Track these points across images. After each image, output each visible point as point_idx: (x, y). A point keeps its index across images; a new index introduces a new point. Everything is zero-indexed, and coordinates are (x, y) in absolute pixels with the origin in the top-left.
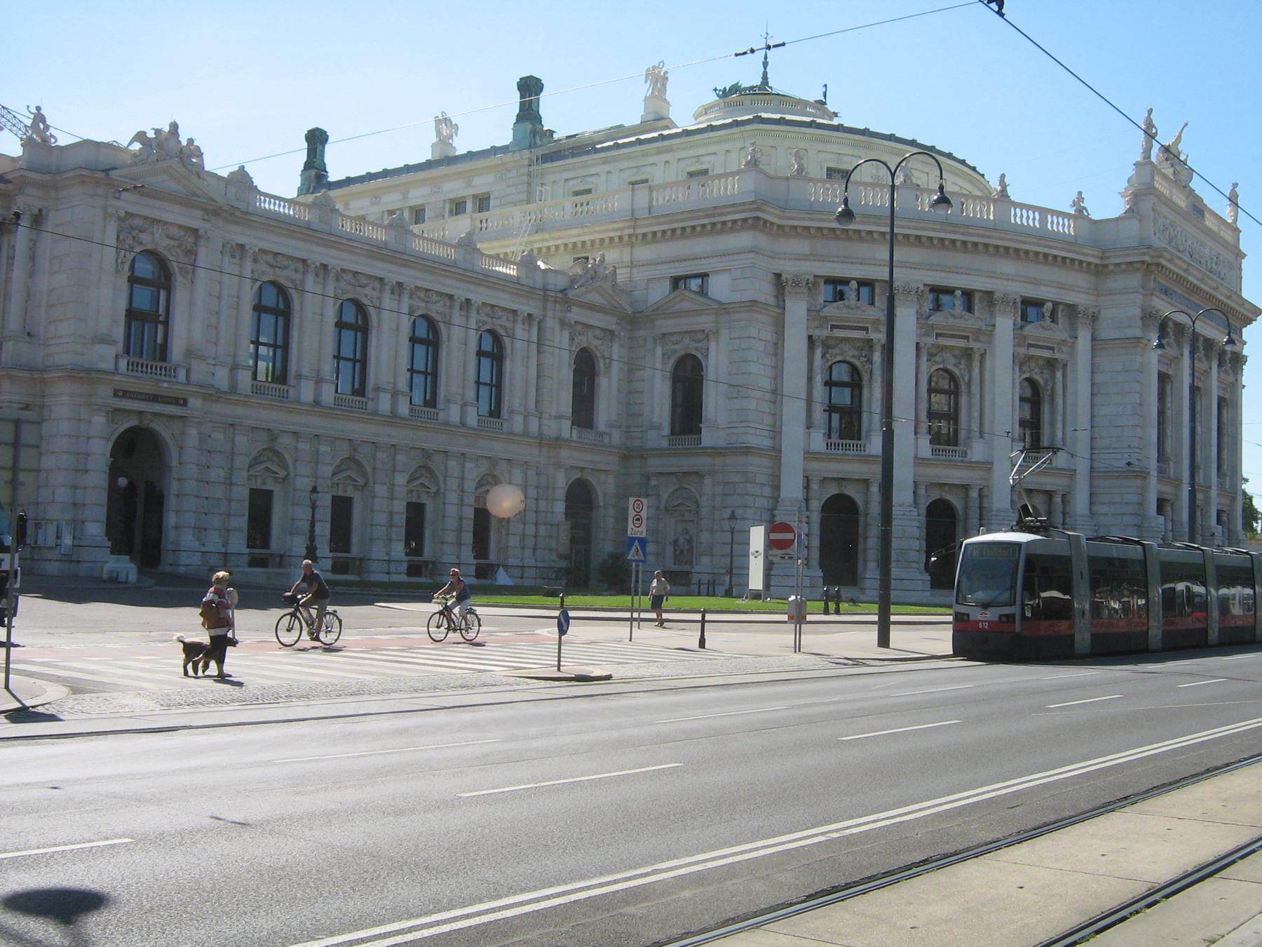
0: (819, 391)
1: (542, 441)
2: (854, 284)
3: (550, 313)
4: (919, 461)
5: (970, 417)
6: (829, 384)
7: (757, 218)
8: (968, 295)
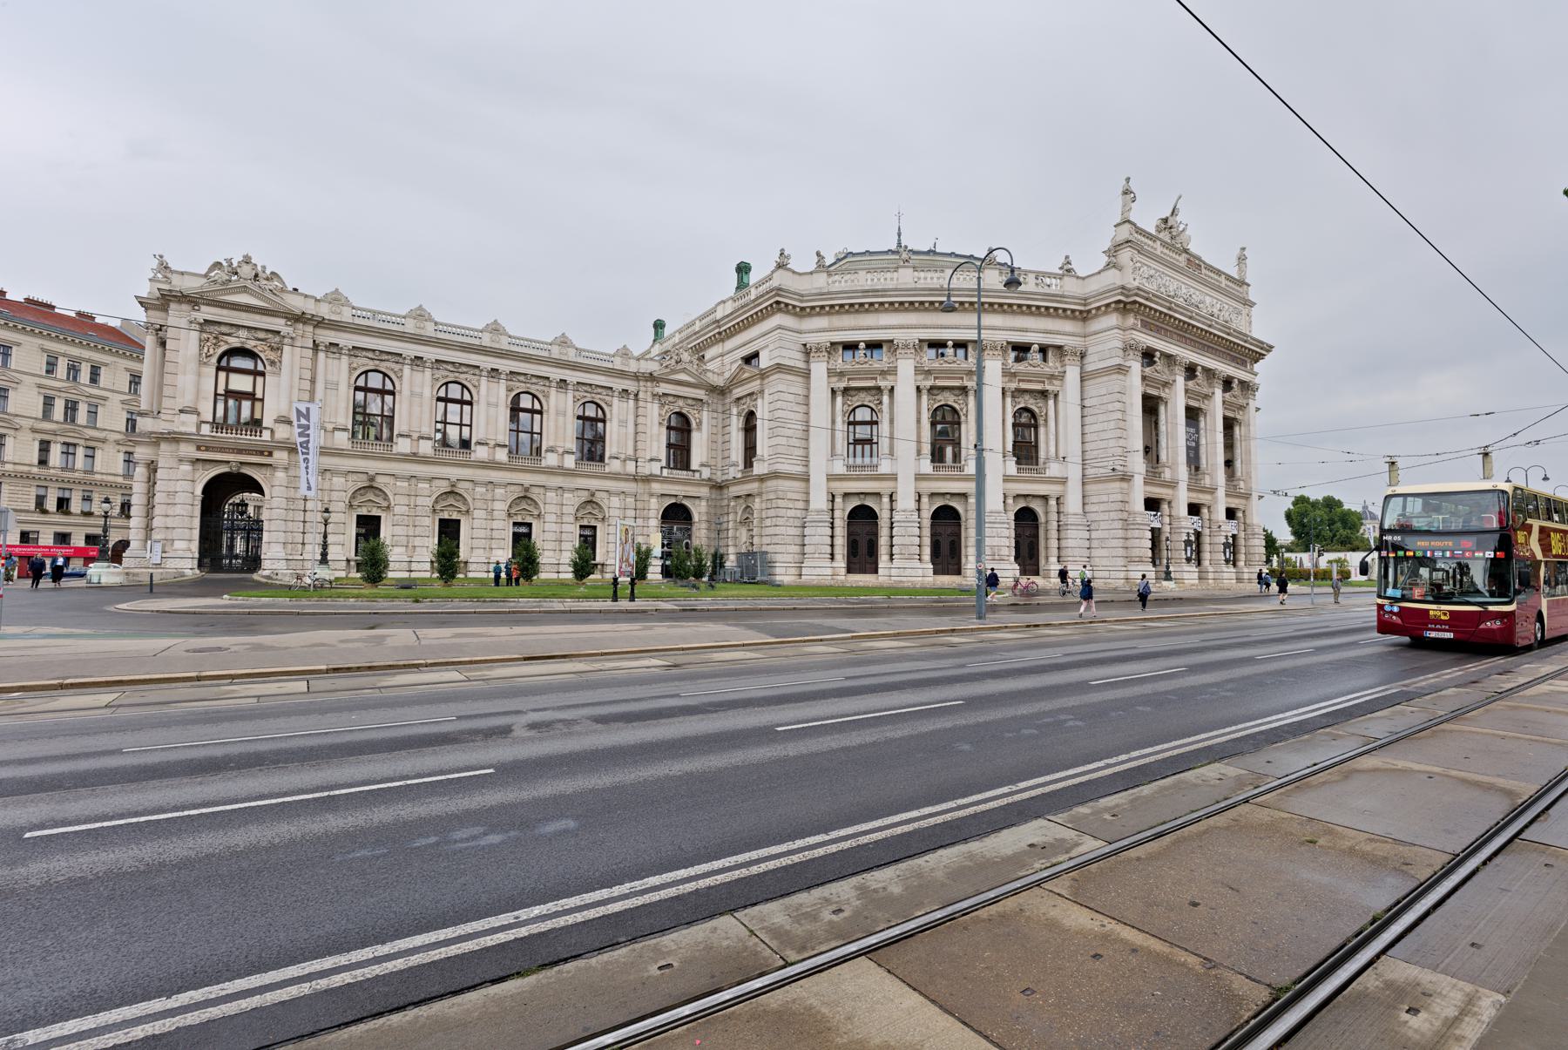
1: (635, 478)
4: (919, 477)
7: (778, 303)
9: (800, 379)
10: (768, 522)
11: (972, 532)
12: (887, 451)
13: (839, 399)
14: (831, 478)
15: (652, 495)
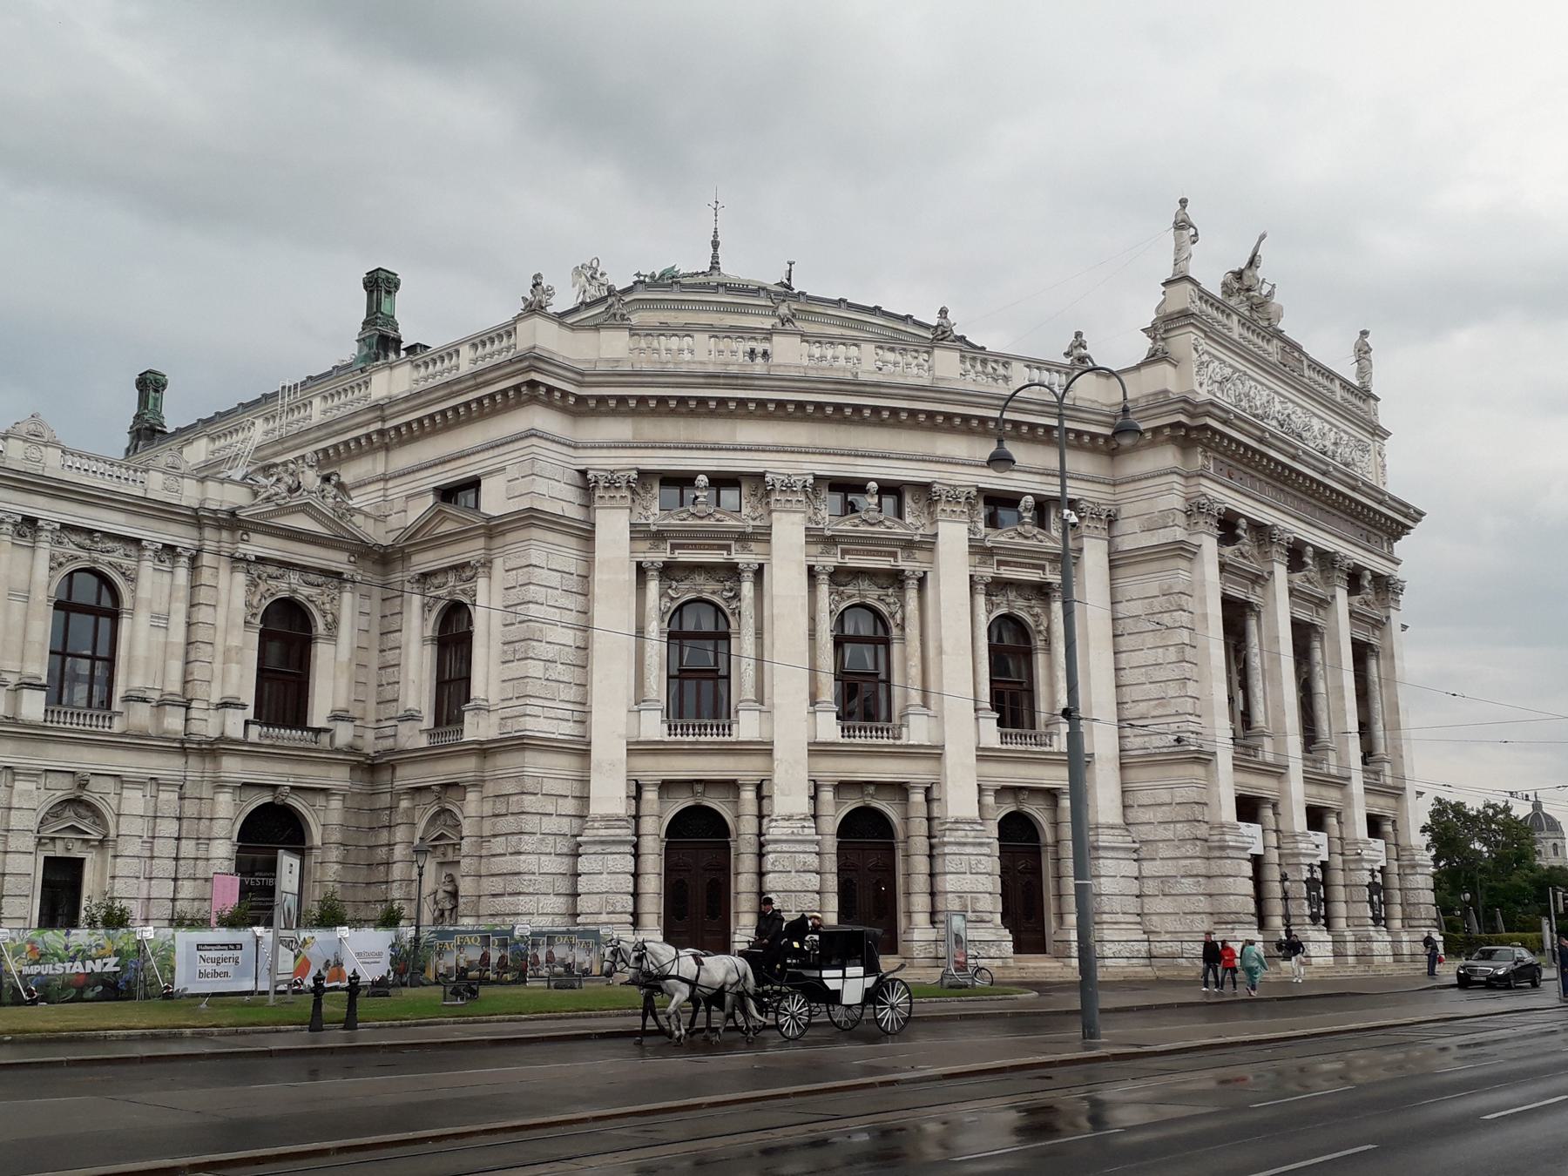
0: (656, 649)
1: (185, 747)
2: (702, 480)
3: (210, 545)
4: (818, 750)
5: (905, 675)
6: (675, 637)
7: (533, 384)
8: (891, 489)
9: (573, 542)
10: (498, 845)
11: (921, 864)
12: (749, 693)
13: (653, 587)
14: (637, 749)
15: (219, 786)
